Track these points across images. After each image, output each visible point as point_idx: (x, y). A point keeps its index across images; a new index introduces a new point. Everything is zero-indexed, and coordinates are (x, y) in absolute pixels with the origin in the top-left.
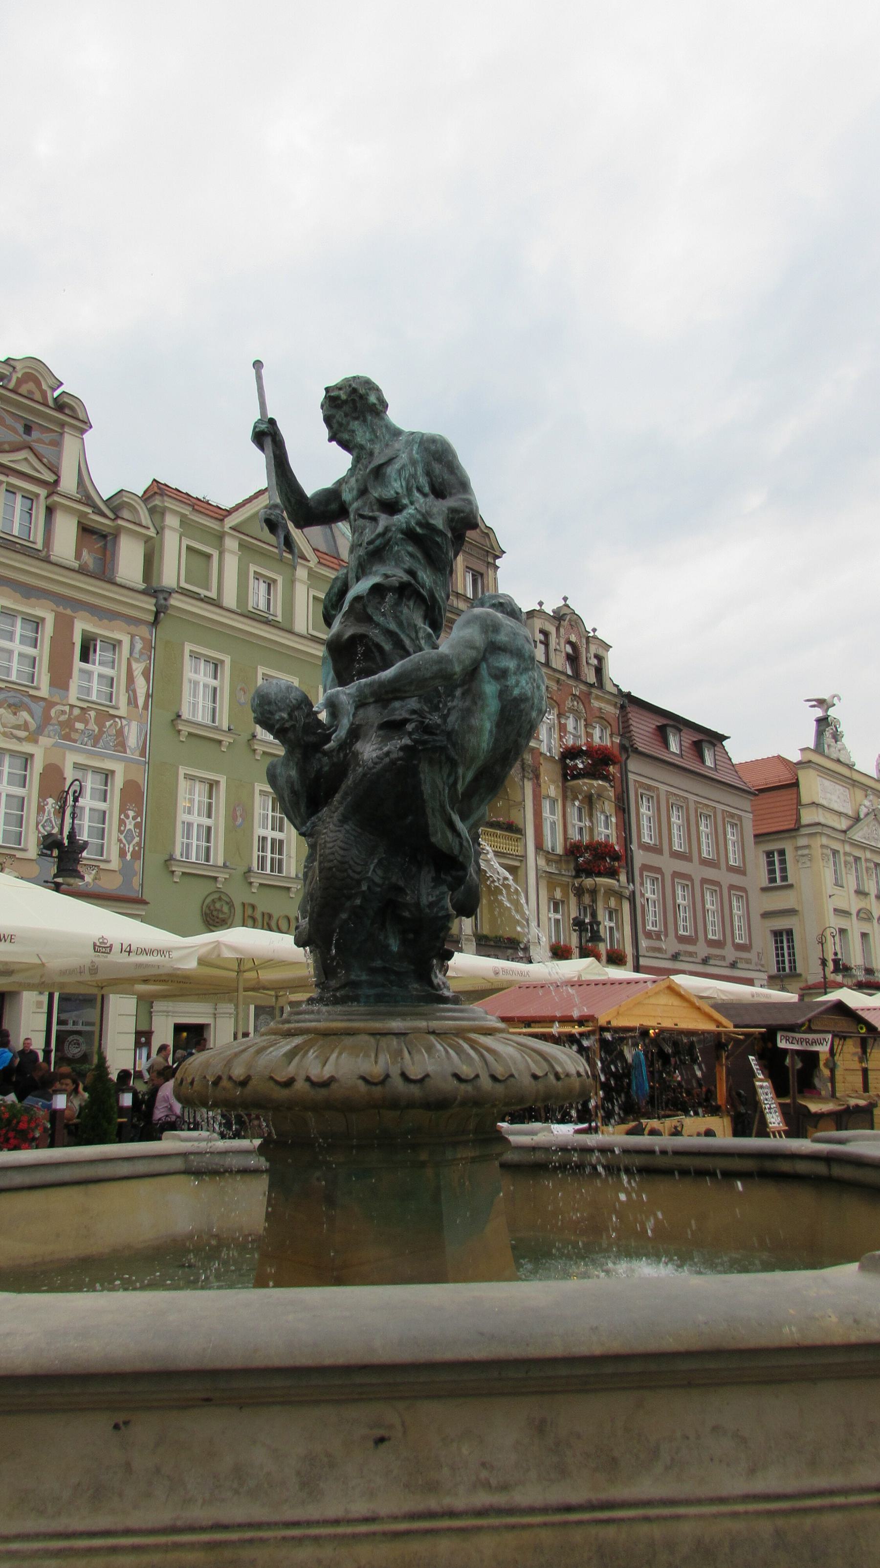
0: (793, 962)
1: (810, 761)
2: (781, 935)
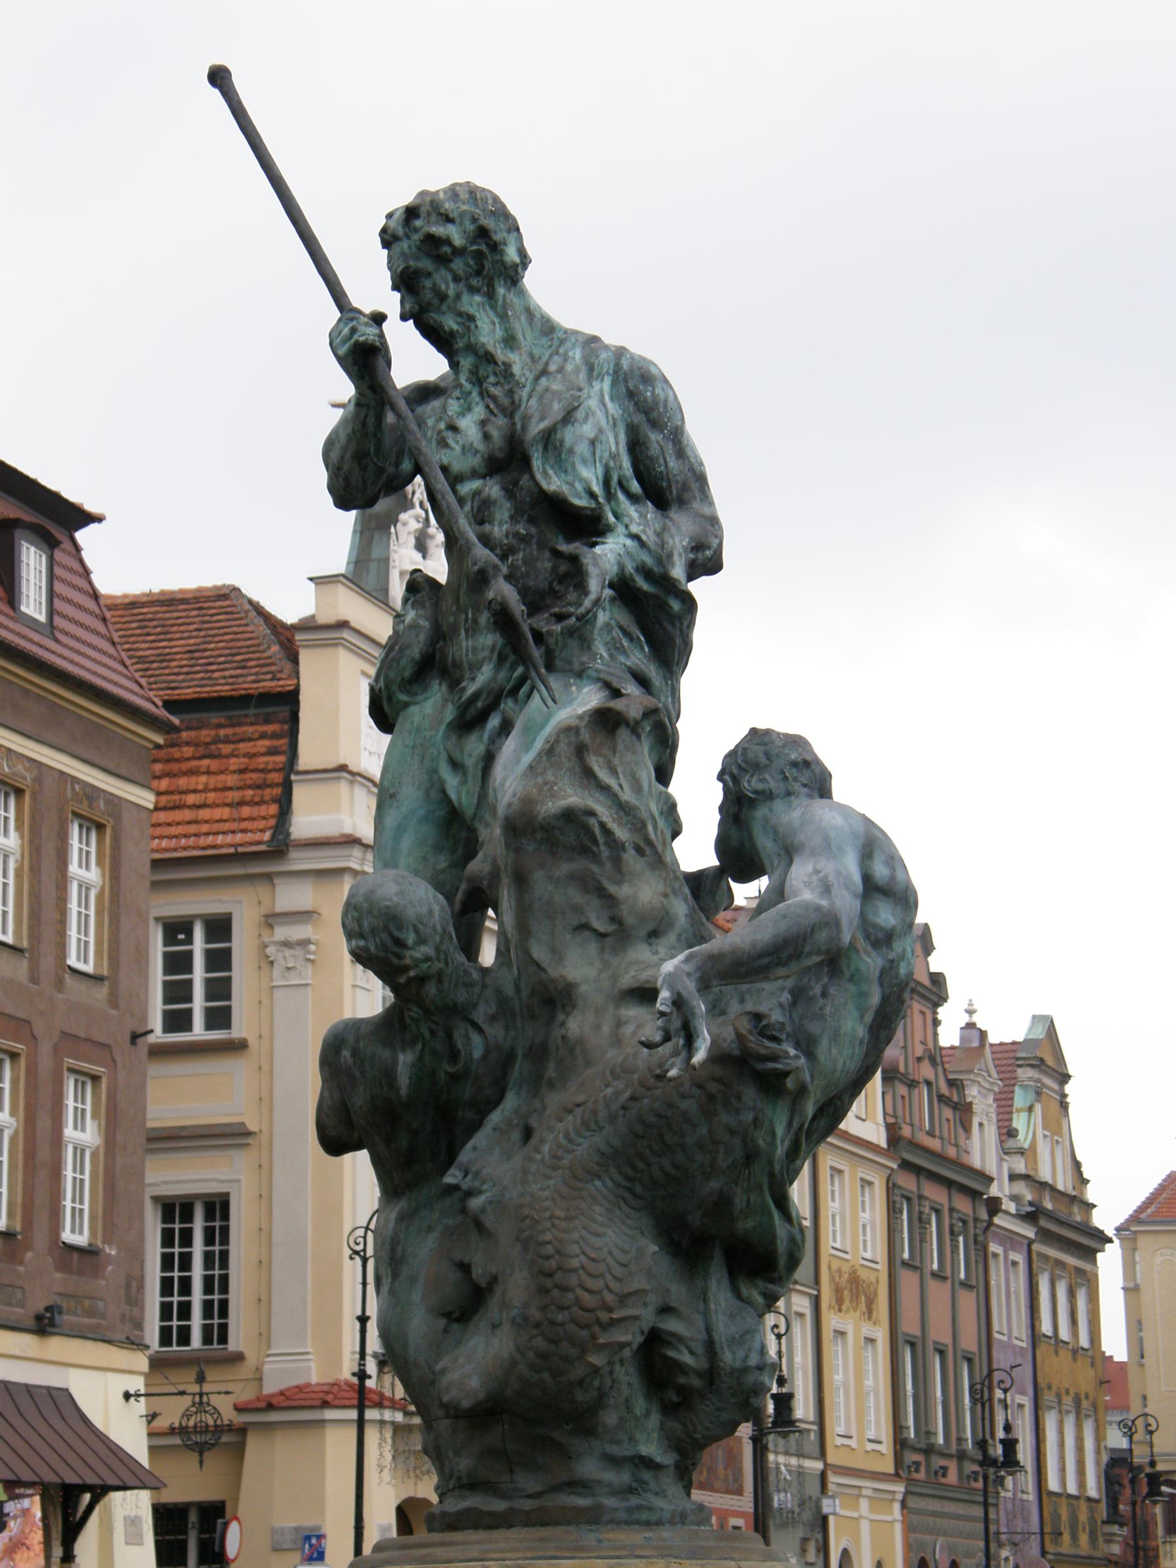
0: (218, 1310)
1: (343, 625)
2: (187, 1216)
